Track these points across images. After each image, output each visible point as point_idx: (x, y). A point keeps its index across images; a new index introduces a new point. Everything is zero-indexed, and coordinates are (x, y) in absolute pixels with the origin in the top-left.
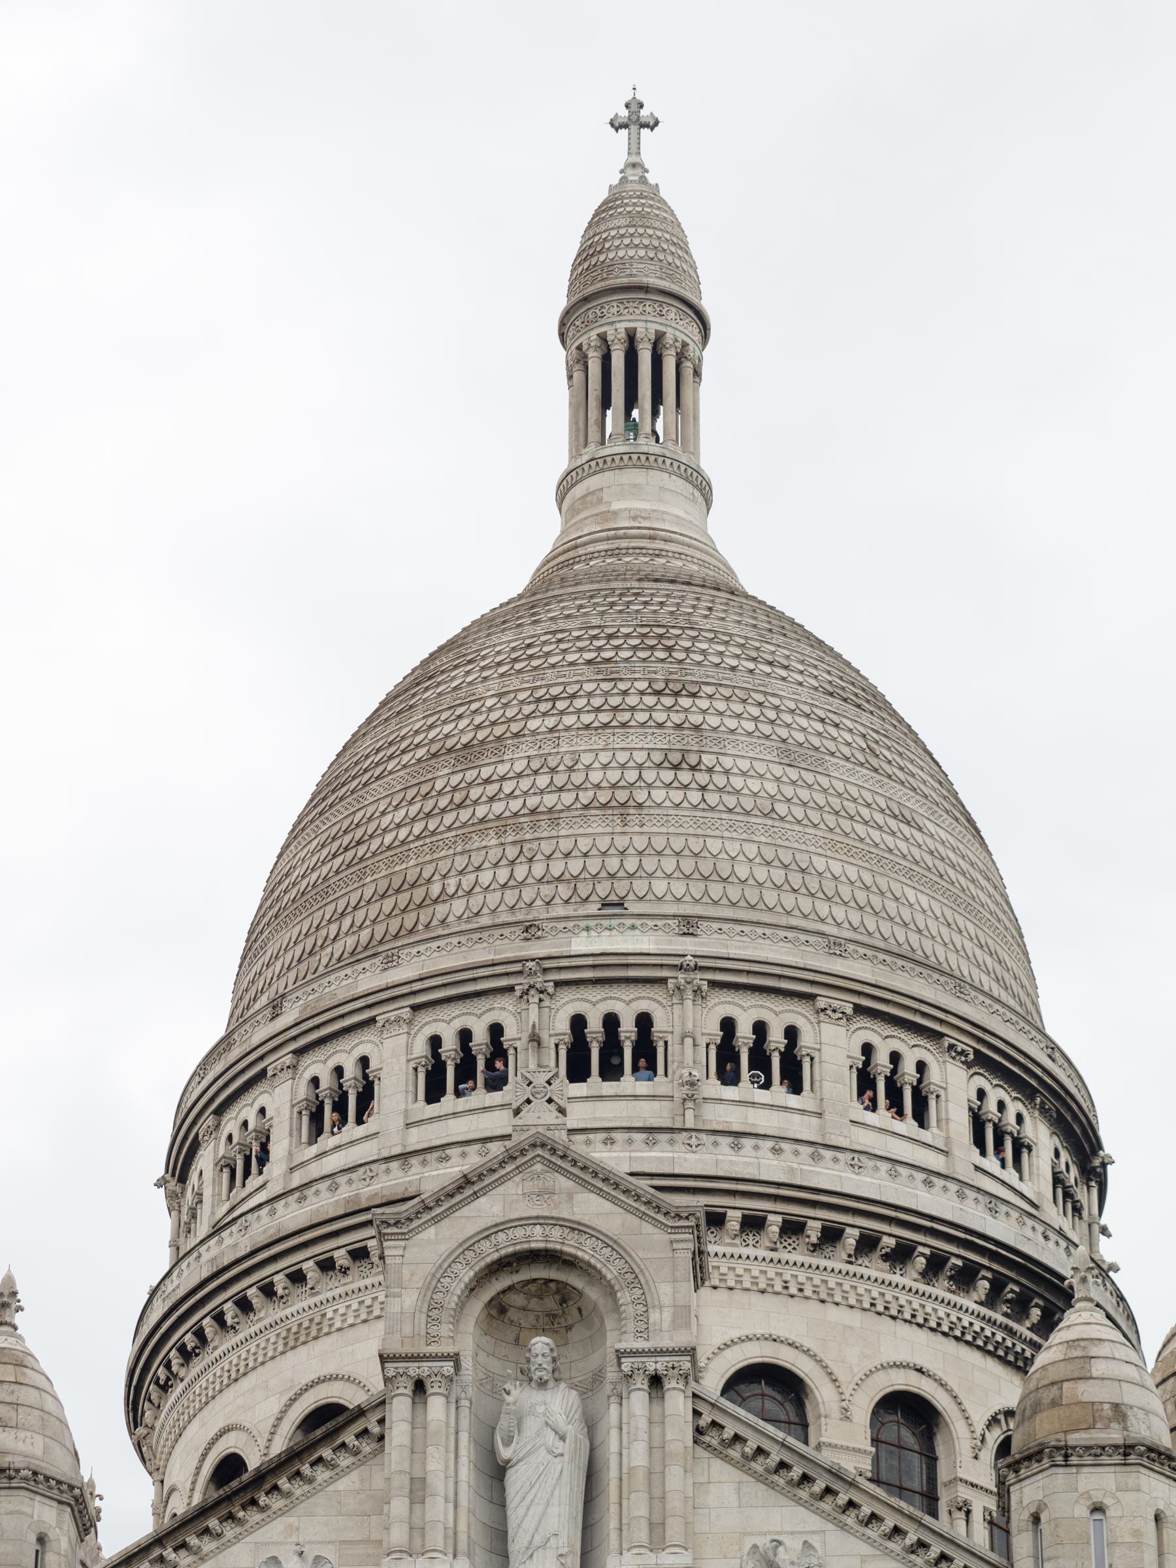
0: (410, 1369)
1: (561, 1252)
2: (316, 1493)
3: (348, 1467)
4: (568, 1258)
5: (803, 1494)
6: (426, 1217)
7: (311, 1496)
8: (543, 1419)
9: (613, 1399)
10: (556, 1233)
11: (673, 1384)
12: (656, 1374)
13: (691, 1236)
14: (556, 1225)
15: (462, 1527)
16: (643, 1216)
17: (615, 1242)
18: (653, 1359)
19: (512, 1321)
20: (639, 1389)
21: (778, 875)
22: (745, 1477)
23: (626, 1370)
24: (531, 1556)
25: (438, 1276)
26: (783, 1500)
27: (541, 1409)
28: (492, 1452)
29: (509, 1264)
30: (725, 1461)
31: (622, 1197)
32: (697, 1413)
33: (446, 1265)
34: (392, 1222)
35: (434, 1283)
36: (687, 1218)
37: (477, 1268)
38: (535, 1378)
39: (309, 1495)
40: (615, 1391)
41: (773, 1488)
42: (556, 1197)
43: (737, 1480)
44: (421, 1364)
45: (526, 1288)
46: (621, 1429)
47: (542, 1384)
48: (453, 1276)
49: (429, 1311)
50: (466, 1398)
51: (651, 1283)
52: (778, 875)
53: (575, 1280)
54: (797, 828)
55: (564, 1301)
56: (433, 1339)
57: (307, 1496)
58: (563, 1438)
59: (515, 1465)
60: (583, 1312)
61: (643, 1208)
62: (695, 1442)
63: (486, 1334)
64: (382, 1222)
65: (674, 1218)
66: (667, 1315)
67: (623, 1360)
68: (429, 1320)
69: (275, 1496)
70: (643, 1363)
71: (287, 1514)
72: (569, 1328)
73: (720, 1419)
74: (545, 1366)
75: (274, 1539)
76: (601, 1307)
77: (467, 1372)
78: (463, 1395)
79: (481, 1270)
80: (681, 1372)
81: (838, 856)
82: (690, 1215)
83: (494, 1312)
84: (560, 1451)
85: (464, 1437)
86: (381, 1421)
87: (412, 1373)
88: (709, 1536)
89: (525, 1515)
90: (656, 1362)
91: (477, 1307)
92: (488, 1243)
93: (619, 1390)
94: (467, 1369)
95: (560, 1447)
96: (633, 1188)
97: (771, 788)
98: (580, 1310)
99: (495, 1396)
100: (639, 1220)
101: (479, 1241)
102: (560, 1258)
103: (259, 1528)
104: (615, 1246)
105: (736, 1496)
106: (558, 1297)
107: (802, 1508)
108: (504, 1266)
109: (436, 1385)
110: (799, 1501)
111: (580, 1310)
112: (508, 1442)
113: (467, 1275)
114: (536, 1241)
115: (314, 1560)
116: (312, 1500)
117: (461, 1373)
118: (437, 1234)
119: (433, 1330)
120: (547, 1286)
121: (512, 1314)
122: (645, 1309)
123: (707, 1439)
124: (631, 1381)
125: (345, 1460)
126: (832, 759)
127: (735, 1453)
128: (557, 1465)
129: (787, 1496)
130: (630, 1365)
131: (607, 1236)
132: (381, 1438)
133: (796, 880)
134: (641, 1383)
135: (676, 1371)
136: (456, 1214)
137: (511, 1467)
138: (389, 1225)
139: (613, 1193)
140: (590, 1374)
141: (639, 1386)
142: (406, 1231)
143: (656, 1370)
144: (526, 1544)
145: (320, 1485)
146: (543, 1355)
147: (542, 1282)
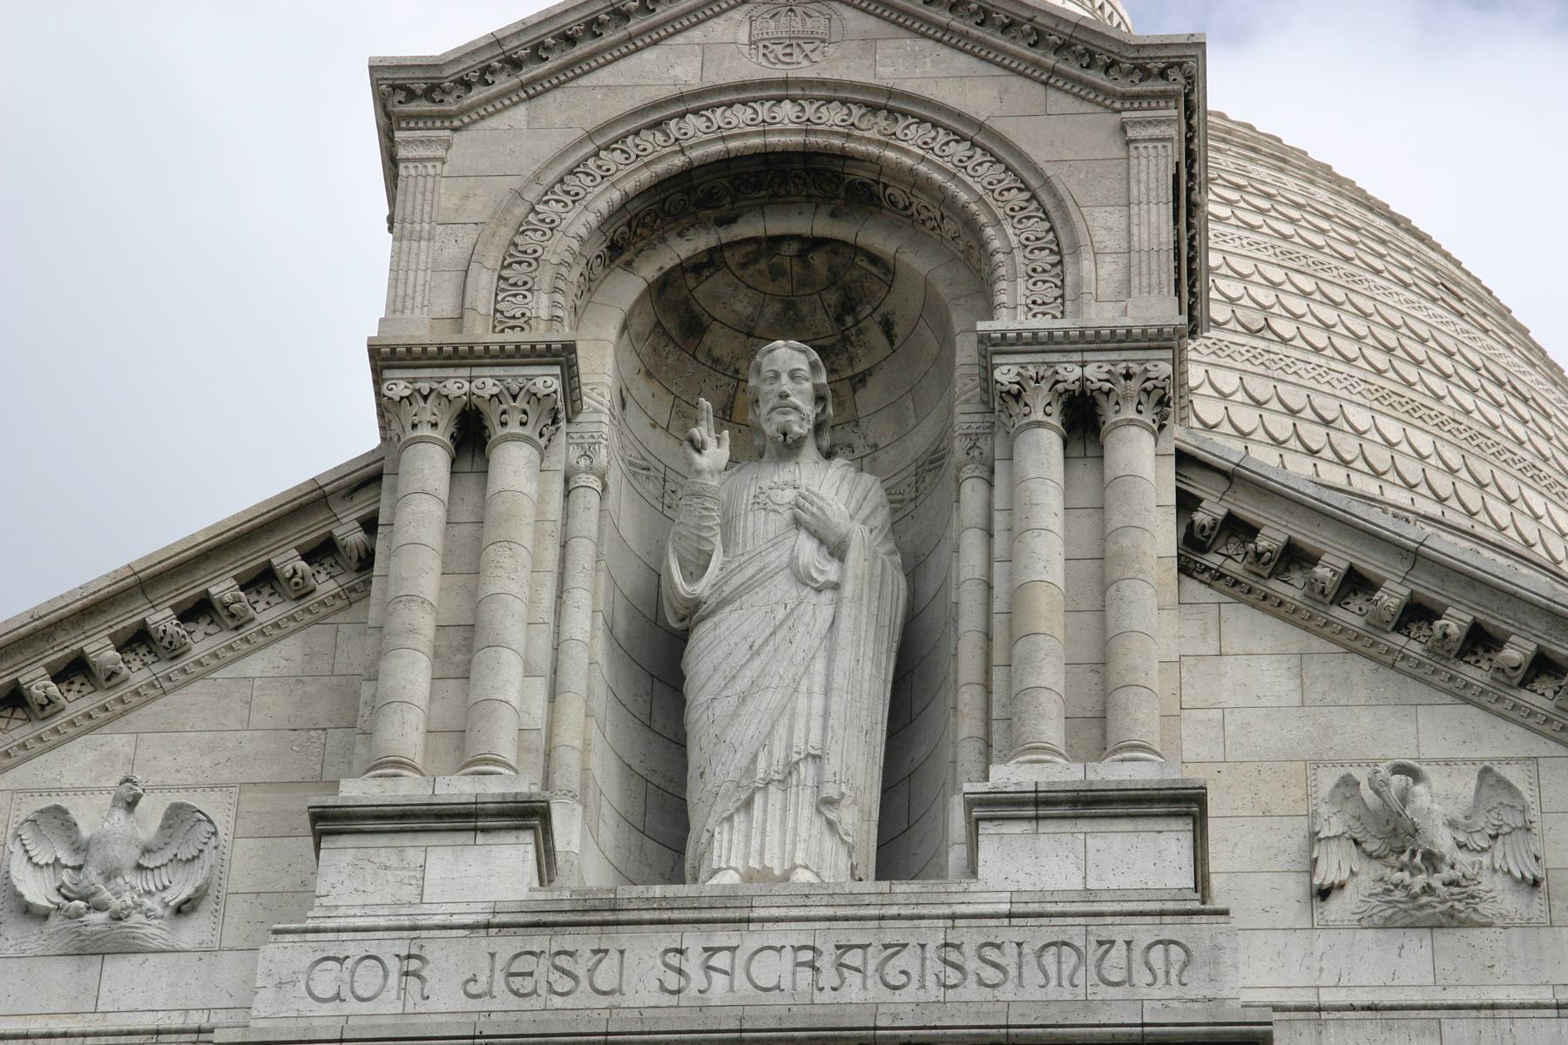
0: (450, 383)
1: (844, 156)
2: (187, 683)
3: (276, 625)
4: (863, 175)
5: (1475, 674)
6: (503, 82)
7: (176, 688)
8: (787, 514)
9: (968, 470)
10: (833, 116)
11: (1129, 413)
12: (1083, 392)
13: (1175, 112)
14: (829, 101)
15: (570, 733)
16: (1049, 79)
17: (981, 127)
18: (1077, 357)
19: (717, 361)
20: (1039, 424)
21: (1281, 426)
22: (1316, 644)
23: (1004, 379)
24: (748, 804)
25: (532, 195)
26: (1417, 691)
27: (789, 495)
28: (656, 578)
29: (709, 200)
30: (1264, 611)
31: (1000, 40)
32: (1186, 503)
33: (551, 177)
34: (419, 87)
35: (520, 211)
36: (1163, 74)
37: (630, 185)
38: (770, 430)
39: (166, 685)
40: (976, 453)
41: (1393, 667)
42: (830, 49)
43: (1295, 648)
44: (476, 371)
45: (751, 269)
46: (990, 535)
47: (789, 448)
48: (568, 199)
49: (503, 267)
50: (590, 470)
51: (1069, 203)
52: (1281, 426)
53: (876, 237)
54: (1314, 359)
55: (848, 306)
56: (512, 323)
57: (161, 688)
58: (837, 551)
59: (712, 613)
60: (897, 330)
61: (1050, 60)
62: (1185, 568)
63: (649, 374)
64: (394, 88)
65: (1130, 73)
66: (1110, 269)
67: (997, 360)
68: (502, 285)
69: (76, 687)
70: (1050, 365)
71: (106, 729)
72: (859, 380)
73: (1248, 510)
74: (793, 399)
75: (66, 782)
76: (942, 290)
77: (595, 417)
78: (583, 463)
79: (642, 193)
80: (1149, 385)
81: (1394, 413)
82: (1171, 66)
83: (670, 324)
84: (833, 577)
85: (583, 552)
86: (370, 525)
87: (452, 388)
88: (1223, 767)
89: (734, 716)
90: (1083, 365)
91: (628, 288)
92: (660, 137)
93: (986, 449)
94: (597, 411)
95: (832, 571)
96: (1028, 14)
97: (1265, 296)
98: (887, 326)
99: (666, 511)
100: (1040, 88)
101: (637, 133)
102: (839, 177)
103: (28, 759)
104: (978, 138)
105: (1294, 684)
106: (832, 297)
107: (1471, 710)
108: (701, 204)
109: (514, 419)
110: (1463, 695)
111: (887, 326)
112: (696, 566)
113: (604, 199)
114: (782, 132)
115: (167, 817)
116: (174, 698)
117: (580, 418)
118: (530, 120)
119: (511, 307)
120: (807, 265)
121: (720, 341)
122: (1055, 258)
123: (1213, 560)
124: (1016, 408)
125: (267, 611)
126: (1376, 279)
127: (1290, 590)
128: (822, 607)
129: (1429, 683)
130: (1015, 370)
131: (960, 116)
132: (366, 561)
133: (1315, 436)
134: (1042, 409)
135: (1134, 385)
136: (584, 81)
137: (703, 619)
138: (411, 95)
139: (977, 32)
140: (913, 468)
141: (1038, 415)
142: (454, 108)
143: (1083, 380)
144: (734, 774)
145: (199, 663)
146: (793, 375)
147: (792, 249)
